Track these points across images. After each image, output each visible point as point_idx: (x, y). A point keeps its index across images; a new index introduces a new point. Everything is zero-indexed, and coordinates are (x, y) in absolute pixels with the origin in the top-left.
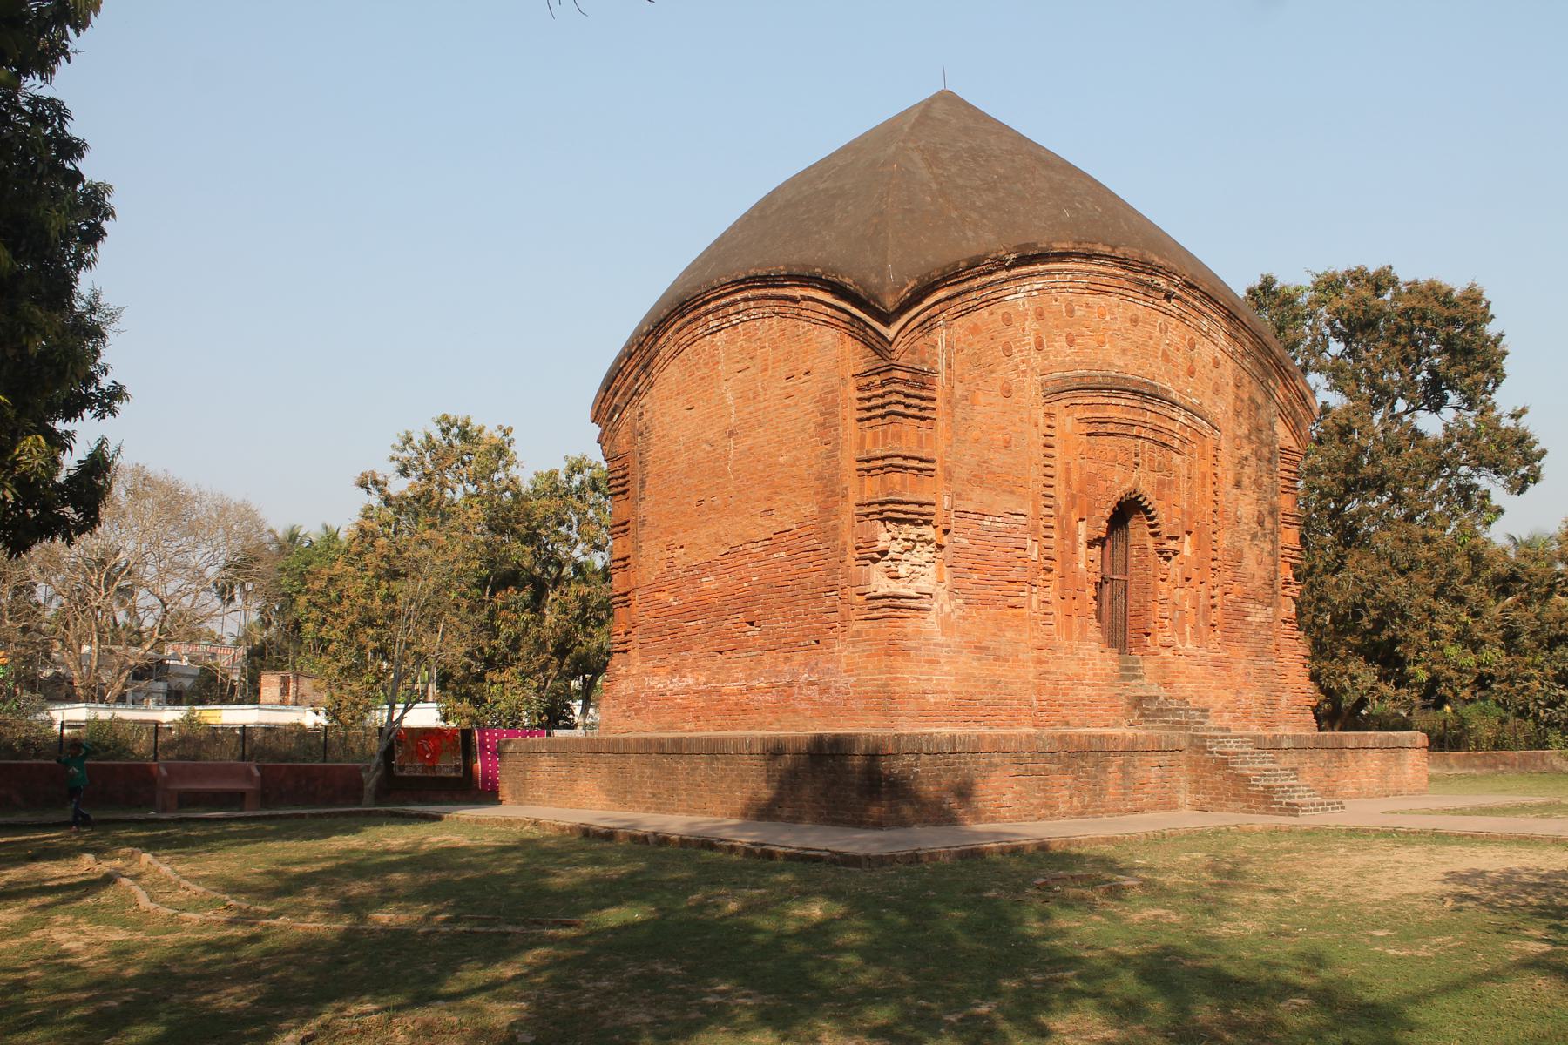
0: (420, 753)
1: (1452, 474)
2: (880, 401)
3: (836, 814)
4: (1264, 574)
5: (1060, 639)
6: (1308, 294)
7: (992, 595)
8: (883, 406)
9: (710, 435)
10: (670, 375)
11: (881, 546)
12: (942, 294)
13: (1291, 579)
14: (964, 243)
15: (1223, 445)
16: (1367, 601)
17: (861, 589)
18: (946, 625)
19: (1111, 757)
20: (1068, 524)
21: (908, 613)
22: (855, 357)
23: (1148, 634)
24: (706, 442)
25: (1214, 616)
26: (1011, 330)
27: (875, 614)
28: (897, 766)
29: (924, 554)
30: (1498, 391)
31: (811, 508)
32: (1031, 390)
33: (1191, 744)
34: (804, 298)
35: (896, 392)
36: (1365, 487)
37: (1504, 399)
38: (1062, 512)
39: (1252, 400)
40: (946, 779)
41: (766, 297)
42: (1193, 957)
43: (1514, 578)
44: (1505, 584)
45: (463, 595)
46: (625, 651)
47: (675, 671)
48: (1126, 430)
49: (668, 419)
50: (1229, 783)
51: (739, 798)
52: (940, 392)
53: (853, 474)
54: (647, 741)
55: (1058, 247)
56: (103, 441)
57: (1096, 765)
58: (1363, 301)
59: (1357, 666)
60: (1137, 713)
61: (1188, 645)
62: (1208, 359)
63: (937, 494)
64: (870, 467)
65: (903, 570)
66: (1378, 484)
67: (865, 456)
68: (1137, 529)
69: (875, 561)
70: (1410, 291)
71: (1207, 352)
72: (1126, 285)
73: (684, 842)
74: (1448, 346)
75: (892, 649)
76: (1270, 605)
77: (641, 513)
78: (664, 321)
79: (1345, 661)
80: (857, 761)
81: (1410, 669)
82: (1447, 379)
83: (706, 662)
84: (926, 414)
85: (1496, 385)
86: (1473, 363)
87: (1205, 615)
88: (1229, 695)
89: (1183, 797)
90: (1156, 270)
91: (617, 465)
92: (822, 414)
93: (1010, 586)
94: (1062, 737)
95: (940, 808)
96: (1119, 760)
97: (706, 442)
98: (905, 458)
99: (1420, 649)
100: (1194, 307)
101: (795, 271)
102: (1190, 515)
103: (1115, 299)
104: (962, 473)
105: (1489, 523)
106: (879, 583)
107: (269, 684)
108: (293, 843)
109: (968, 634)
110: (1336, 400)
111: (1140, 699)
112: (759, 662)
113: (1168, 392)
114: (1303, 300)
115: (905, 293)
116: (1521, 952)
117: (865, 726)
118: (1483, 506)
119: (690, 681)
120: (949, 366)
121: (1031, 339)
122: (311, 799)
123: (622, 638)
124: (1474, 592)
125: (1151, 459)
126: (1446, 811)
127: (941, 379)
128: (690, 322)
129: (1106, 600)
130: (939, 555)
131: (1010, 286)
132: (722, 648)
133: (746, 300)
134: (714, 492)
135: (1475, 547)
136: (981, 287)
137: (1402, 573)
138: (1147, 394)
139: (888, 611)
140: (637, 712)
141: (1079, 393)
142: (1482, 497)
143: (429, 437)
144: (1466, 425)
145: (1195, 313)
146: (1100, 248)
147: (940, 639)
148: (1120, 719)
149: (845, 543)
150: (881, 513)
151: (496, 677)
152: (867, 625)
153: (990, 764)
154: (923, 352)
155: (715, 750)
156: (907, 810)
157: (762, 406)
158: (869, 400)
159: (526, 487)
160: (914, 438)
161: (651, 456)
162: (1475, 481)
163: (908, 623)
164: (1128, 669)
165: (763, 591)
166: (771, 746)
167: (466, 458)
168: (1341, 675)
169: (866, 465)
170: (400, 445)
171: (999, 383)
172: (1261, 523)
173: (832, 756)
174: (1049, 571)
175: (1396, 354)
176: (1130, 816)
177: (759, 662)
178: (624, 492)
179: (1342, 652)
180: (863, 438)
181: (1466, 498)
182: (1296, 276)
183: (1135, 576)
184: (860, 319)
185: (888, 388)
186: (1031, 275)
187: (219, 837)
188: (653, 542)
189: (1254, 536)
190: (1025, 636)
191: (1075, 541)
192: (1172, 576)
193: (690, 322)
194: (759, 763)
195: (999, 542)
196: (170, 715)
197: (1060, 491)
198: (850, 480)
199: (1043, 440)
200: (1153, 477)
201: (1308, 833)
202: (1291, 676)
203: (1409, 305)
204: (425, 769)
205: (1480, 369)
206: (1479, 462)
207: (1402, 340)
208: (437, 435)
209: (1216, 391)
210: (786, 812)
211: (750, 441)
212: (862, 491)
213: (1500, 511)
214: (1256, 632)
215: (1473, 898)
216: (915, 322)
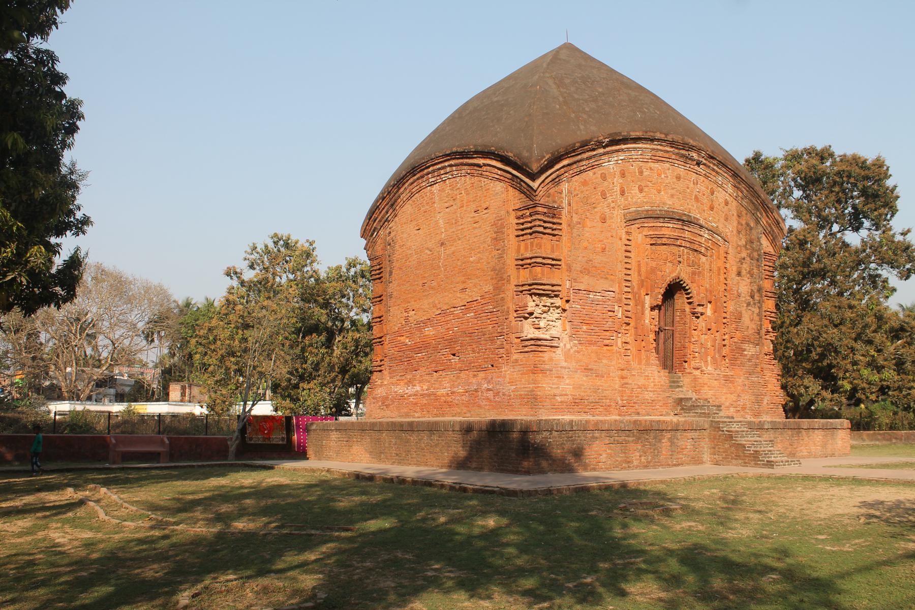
0: (261, 430)
1: (865, 268)
2: (529, 225)
3: (503, 466)
4: (754, 326)
5: (634, 364)
6: (781, 162)
7: (594, 338)
8: (531, 228)
9: (430, 245)
10: (407, 210)
11: (529, 310)
12: (565, 162)
13: (770, 329)
14: (578, 133)
15: (730, 251)
16: (816, 343)
17: (518, 335)
18: (568, 356)
19: (664, 433)
20: (639, 297)
21: (545, 349)
22: (515, 199)
23: (686, 362)
24: (428, 249)
25: (725, 351)
26: (606, 183)
27: (526, 349)
28: (539, 438)
29: (554, 314)
30: (894, 219)
31: (489, 288)
32: (617, 218)
33: (711, 426)
34: (485, 165)
35: (538, 219)
36: (814, 276)
37: (897, 224)
38: (636, 290)
39: (748, 224)
40: (568, 446)
41: (462, 164)
42: (711, 550)
43: (902, 329)
44: (896, 333)
45: (286, 338)
46: (380, 371)
47: (410, 382)
48: (673, 242)
49: (405, 236)
50: (733, 449)
51: (447, 456)
52: (564, 220)
53: (513, 268)
54: (393, 424)
55: (634, 134)
56: (78, 249)
57: (655, 438)
58: (814, 166)
59: (809, 381)
60: (679, 408)
61: (709, 368)
62: (721, 200)
63: (561, 279)
64: (523, 263)
65: (542, 324)
66: (821, 274)
67: (520, 257)
68: (680, 300)
69: (526, 318)
70: (841, 161)
71: (721, 196)
72: (673, 157)
73: (414, 482)
74: (864, 193)
75: (536, 370)
76: (757, 345)
77: (389, 290)
78: (403, 178)
79: (802, 378)
80: (515, 435)
81: (840, 382)
82: (863, 212)
83: (427, 377)
84: (556, 232)
85: (892, 216)
86: (879, 203)
87: (719, 351)
88: (733, 397)
89: (706, 457)
90: (692, 148)
91: (375, 262)
92: (495, 232)
93: (605, 333)
94: (635, 422)
95: (564, 463)
96: (668, 435)
97: (428, 249)
98: (544, 258)
99: (846, 371)
100: (713, 170)
101: (480, 149)
102: (711, 292)
103: (667, 165)
104: (577, 267)
105: (887, 297)
106: (529, 331)
107: (174, 390)
108: (188, 482)
109: (580, 361)
110: (797, 225)
111: (681, 399)
112: (458, 377)
113: (698, 219)
114: (778, 166)
115: (544, 162)
116: (905, 549)
117: (520, 415)
118: (884, 287)
119: (418, 388)
120: (569, 205)
122: (199, 457)
123: (379, 363)
124: (879, 338)
125: (688, 259)
126: (861, 466)
127: (565, 212)
128: (418, 179)
129: (661, 341)
130: (564, 315)
131: (606, 158)
132: (437, 369)
133: (451, 166)
134: (432, 278)
135: (879, 311)
136: (588, 159)
137: (836, 326)
138: (686, 221)
139: (534, 348)
140: (387, 406)
142: (883, 282)
143: (266, 246)
144: (874, 239)
145: (714, 173)
146: (658, 135)
147: (564, 364)
148: (669, 411)
149: (508, 308)
150: (529, 290)
151: (305, 385)
152: (521, 356)
153: (593, 437)
154: (554, 196)
155: (432, 428)
156: (544, 464)
157: (460, 228)
158: (523, 224)
159: (323, 275)
160: (549, 247)
161: (395, 258)
162: (880, 272)
163: (545, 355)
164: (674, 382)
165: (461, 336)
166: (465, 426)
167: (288, 258)
168: (799, 386)
169: (521, 262)
170: (250, 251)
171: (599, 214)
172: (752, 297)
173: (501, 432)
174: (628, 324)
175: (833, 197)
176: (675, 468)
177: (458, 377)
178: (380, 278)
179: (800, 372)
180: (519, 246)
181: (874, 282)
182: (773, 152)
183: (678, 328)
184: (517, 177)
185: (534, 217)
186: (618, 151)
187: (146, 479)
188: (397, 308)
189: (748, 304)
190: (614, 363)
191: (643, 307)
192: (700, 327)
193: (418, 179)
194: (458, 436)
195: (599, 307)
196: (117, 408)
197: (634, 277)
198: (512, 271)
199: (625, 248)
200: (689, 269)
201: (780, 478)
202: (770, 386)
203: (841, 169)
204: (264, 439)
205: (882, 206)
206: (882, 261)
207: (837, 189)
208: (271, 245)
209: (726, 219)
210: (474, 465)
211: (453, 249)
212: (518, 278)
213: (894, 290)
214: (749, 360)
215: (876, 517)
216: (550, 179)
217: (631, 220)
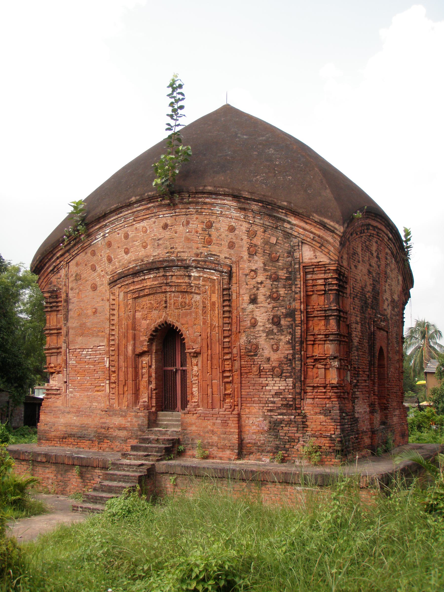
26: (95, 258)
103: (153, 220)
121: (105, 259)
141: (126, 279)
146: (133, 199)
160: (55, 320)
163: (50, 400)
217: (113, 283)
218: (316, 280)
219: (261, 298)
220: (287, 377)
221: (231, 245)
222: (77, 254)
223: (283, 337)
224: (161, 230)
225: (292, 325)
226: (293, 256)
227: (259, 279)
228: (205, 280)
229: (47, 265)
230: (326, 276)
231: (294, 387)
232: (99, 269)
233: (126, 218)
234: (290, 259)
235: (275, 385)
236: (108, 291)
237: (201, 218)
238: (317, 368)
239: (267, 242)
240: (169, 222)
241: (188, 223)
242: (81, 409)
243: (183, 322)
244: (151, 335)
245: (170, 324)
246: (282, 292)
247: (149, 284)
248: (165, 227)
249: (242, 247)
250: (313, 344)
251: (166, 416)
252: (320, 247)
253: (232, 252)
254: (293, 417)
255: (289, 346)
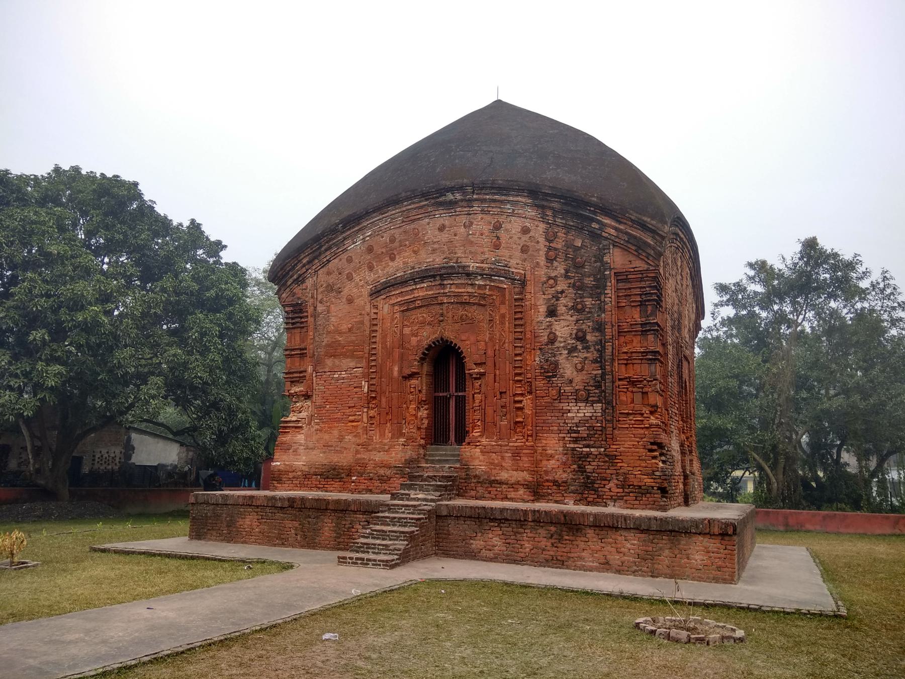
26: (352, 265)
71: (513, 226)
160: (298, 338)
216: (291, 280)
217: (376, 293)
218: (630, 289)
219: (561, 309)
220: (593, 402)
221: (524, 250)
222: (329, 261)
223: (588, 355)
224: (437, 232)
225: (601, 340)
226: (601, 261)
227: (559, 288)
228: (492, 288)
229: (291, 273)
230: (643, 284)
231: (604, 411)
232: (357, 278)
233: (392, 219)
234: (599, 264)
235: (579, 412)
236: (368, 304)
237: (488, 218)
238: (632, 392)
239: (569, 245)
240: (447, 223)
241: (471, 224)
242: (330, 443)
243: (463, 338)
244: (424, 354)
245: (447, 341)
246: (588, 302)
247: (421, 294)
248: (442, 229)
249: (539, 250)
250: (626, 364)
251: (437, 450)
252: (636, 251)
253: (525, 256)
254: (603, 450)
255: (598, 365)
